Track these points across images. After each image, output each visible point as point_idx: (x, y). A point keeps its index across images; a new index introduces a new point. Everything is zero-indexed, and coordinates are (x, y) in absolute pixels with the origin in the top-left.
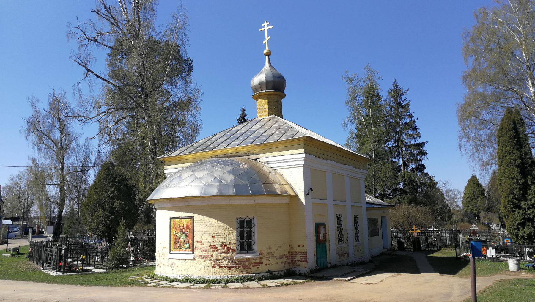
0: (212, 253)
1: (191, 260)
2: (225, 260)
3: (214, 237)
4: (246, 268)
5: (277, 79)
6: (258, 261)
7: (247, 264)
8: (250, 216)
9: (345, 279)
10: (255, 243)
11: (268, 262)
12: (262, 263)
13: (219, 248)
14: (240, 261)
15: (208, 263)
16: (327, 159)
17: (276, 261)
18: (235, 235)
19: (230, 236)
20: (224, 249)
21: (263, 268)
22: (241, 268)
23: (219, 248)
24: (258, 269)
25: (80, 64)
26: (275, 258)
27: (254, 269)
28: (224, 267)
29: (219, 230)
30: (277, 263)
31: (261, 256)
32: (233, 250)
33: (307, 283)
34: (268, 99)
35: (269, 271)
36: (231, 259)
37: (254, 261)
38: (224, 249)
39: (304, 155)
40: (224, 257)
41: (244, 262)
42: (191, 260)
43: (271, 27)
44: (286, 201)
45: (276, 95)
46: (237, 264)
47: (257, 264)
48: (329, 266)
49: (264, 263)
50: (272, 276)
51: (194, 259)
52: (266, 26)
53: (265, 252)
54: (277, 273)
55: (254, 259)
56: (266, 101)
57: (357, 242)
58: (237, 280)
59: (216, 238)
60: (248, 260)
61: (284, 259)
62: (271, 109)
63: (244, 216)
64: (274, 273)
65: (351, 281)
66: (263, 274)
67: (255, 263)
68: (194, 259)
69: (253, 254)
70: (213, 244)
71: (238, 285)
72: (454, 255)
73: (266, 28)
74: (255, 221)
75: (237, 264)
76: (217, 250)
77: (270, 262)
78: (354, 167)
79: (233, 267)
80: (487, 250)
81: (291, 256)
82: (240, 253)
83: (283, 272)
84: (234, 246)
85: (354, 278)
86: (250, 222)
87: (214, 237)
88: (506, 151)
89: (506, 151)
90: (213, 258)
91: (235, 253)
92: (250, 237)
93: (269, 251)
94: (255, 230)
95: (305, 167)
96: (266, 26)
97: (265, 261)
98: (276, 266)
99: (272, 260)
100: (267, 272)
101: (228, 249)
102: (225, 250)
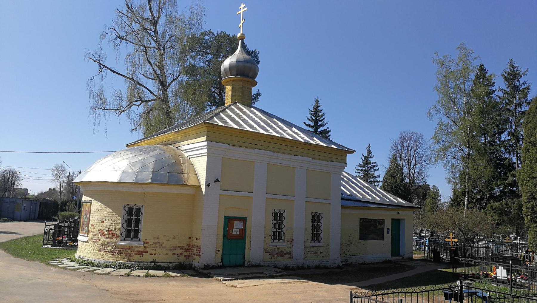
0: (100, 237)
1: (85, 242)
2: (110, 246)
3: (103, 222)
4: (128, 256)
5: (240, 64)
6: (141, 250)
7: (129, 251)
8: (139, 205)
9: (219, 278)
10: (141, 231)
11: (153, 252)
12: (147, 252)
13: (106, 233)
14: (122, 248)
15: (96, 247)
16: (254, 148)
17: (165, 252)
18: (120, 221)
19: (117, 222)
20: (109, 234)
21: (147, 257)
22: (123, 255)
23: (106, 233)
24: (141, 258)
25: (95, 61)
26: (165, 249)
27: (137, 257)
28: (108, 252)
29: (108, 215)
30: (167, 254)
31: (146, 245)
32: (117, 237)
33: (182, 278)
34: (232, 85)
35: (154, 262)
36: (114, 245)
37: (137, 249)
38: (109, 234)
39: (205, 143)
40: (109, 243)
41: (126, 249)
42: (85, 242)
43: (246, 9)
44: (191, 191)
45: (241, 80)
46: (119, 251)
47: (141, 253)
48: (246, 264)
49: (149, 253)
50: (157, 267)
51: (87, 242)
52: (242, 9)
53: (151, 241)
54: (163, 264)
55: (137, 247)
56: (231, 87)
57: (317, 244)
58: (120, 267)
59: (104, 224)
60: (130, 247)
61: (179, 251)
62: (235, 96)
63: (132, 204)
64: (159, 264)
65: (224, 282)
66: (146, 263)
67: (139, 251)
68: (87, 242)
69: (137, 242)
70: (101, 228)
71: (143, 273)
72: (452, 272)
73: (241, 11)
74: (143, 210)
75: (119, 251)
76: (104, 235)
77: (156, 252)
78: (313, 159)
79: (115, 253)
80: (497, 270)
81: (189, 248)
82: (124, 240)
83: (174, 264)
84: (118, 232)
85: (237, 279)
86: (138, 212)
87: (103, 222)
88: (530, 143)
89: (530, 143)
90: (100, 242)
91: (118, 239)
92: (137, 223)
93: (156, 241)
94: (142, 218)
95: (209, 154)
96: (242, 9)
97: (149, 250)
98: (162, 258)
99: (158, 251)
100: (151, 262)
101: (113, 235)
102: (110, 236)
